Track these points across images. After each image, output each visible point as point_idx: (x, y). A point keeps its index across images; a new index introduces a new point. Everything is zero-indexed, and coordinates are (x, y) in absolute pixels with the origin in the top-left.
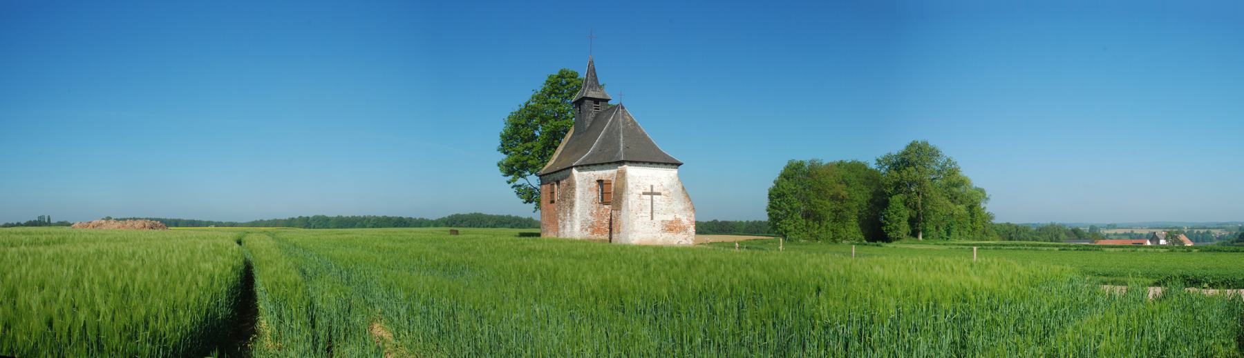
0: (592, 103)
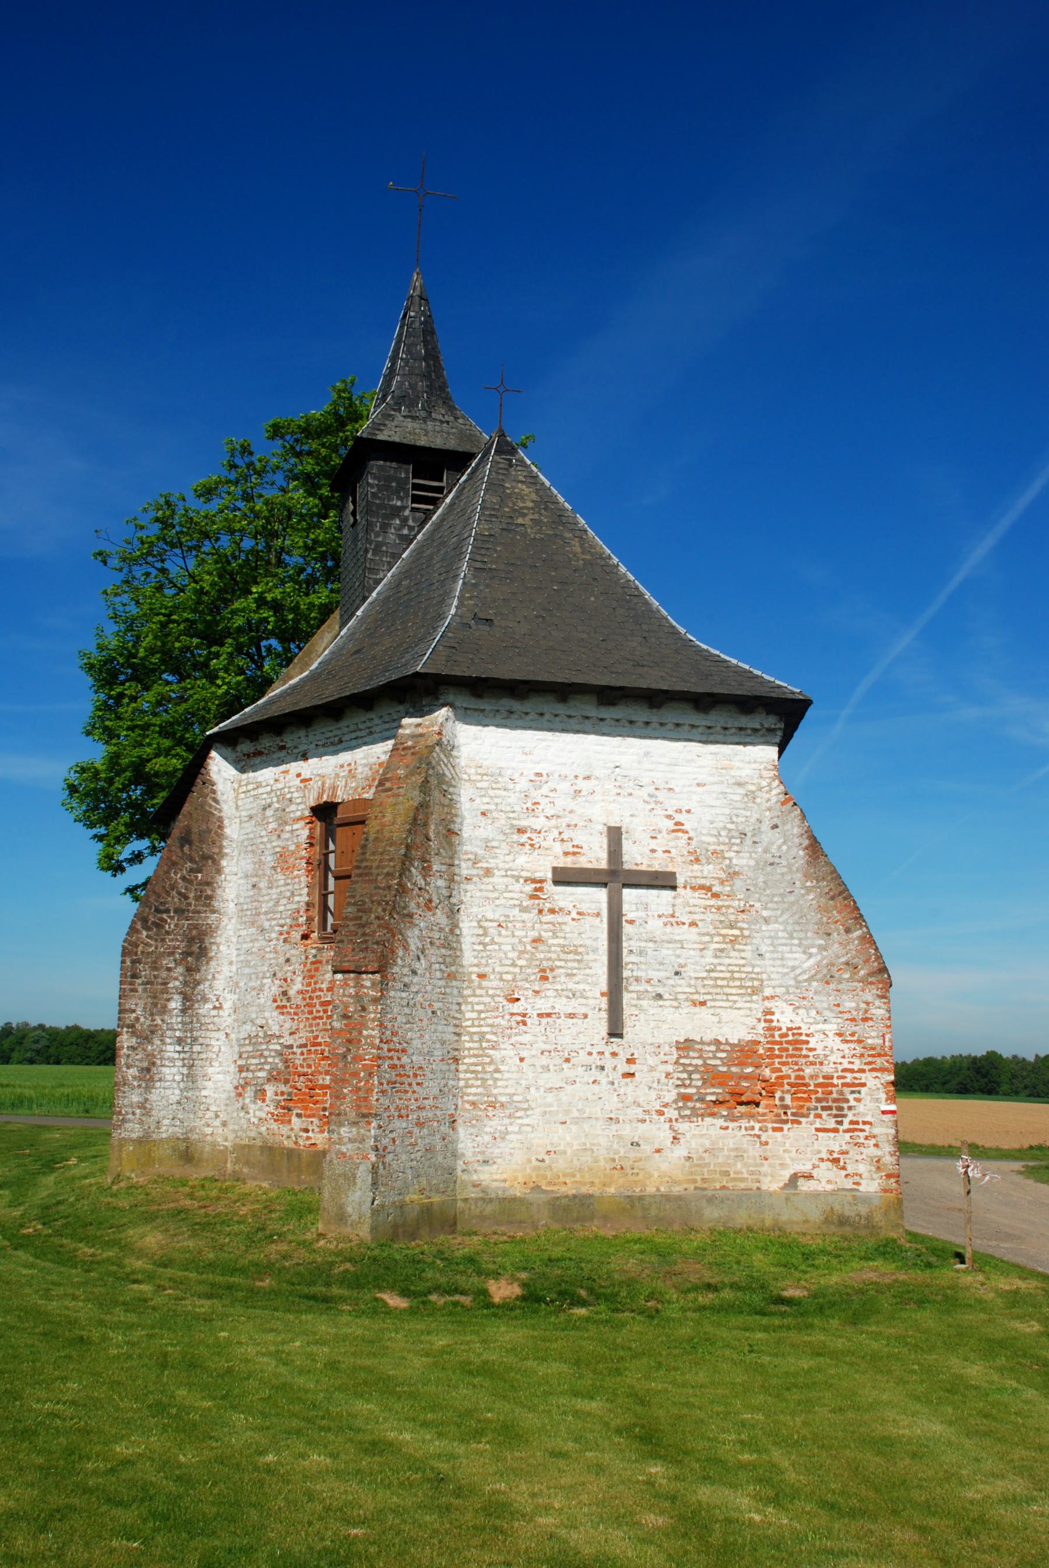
0: (405, 473)
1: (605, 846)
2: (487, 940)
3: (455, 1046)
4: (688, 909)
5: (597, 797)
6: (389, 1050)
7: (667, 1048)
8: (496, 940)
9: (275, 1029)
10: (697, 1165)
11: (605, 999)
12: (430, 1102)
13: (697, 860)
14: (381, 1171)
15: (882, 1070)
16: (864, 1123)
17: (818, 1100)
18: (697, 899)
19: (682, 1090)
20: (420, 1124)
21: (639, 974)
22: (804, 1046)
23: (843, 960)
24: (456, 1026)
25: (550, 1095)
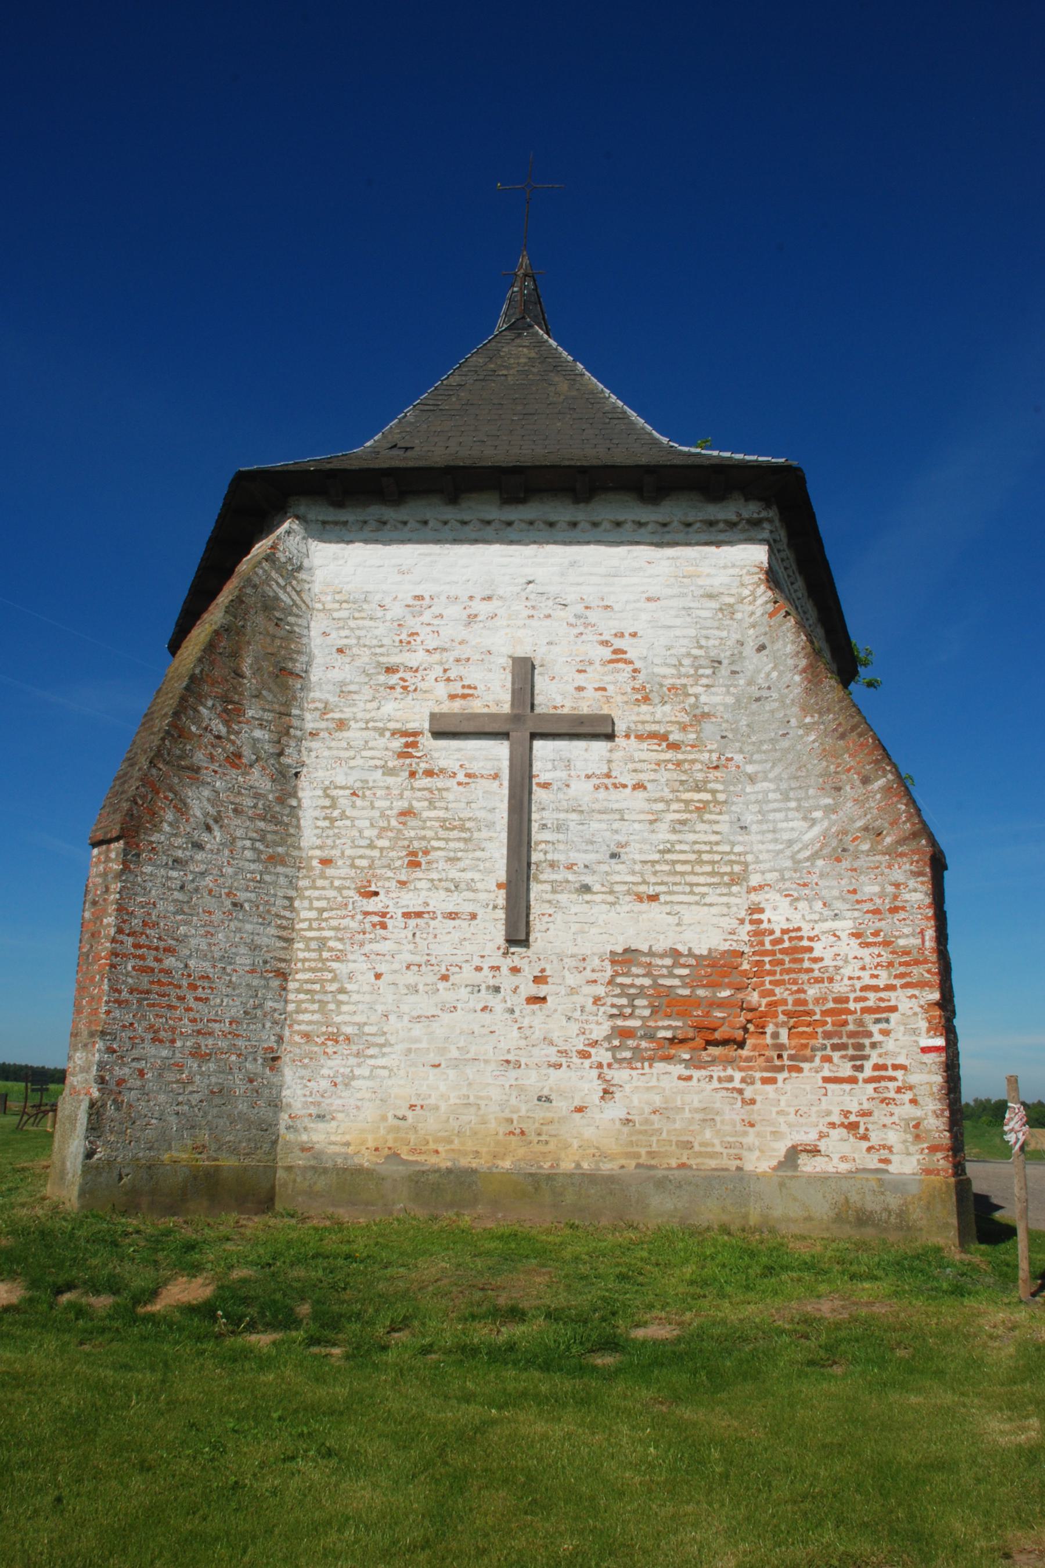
1: (509, 685)
2: (336, 813)
3: (281, 954)
4: (630, 766)
5: (498, 622)
6: (137, 946)
7: (596, 962)
8: (348, 813)
10: (640, 1132)
11: (503, 893)
12: (226, 1028)
13: (646, 699)
14: (110, 1110)
15: (921, 985)
16: (896, 1067)
17: (827, 1035)
18: (646, 752)
19: (620, 1022)
20: (196, 1053)
21: (556, 857)
22: (806, 956)
23: (860, 824)
24: (280, 927)
25: (418, 1025)
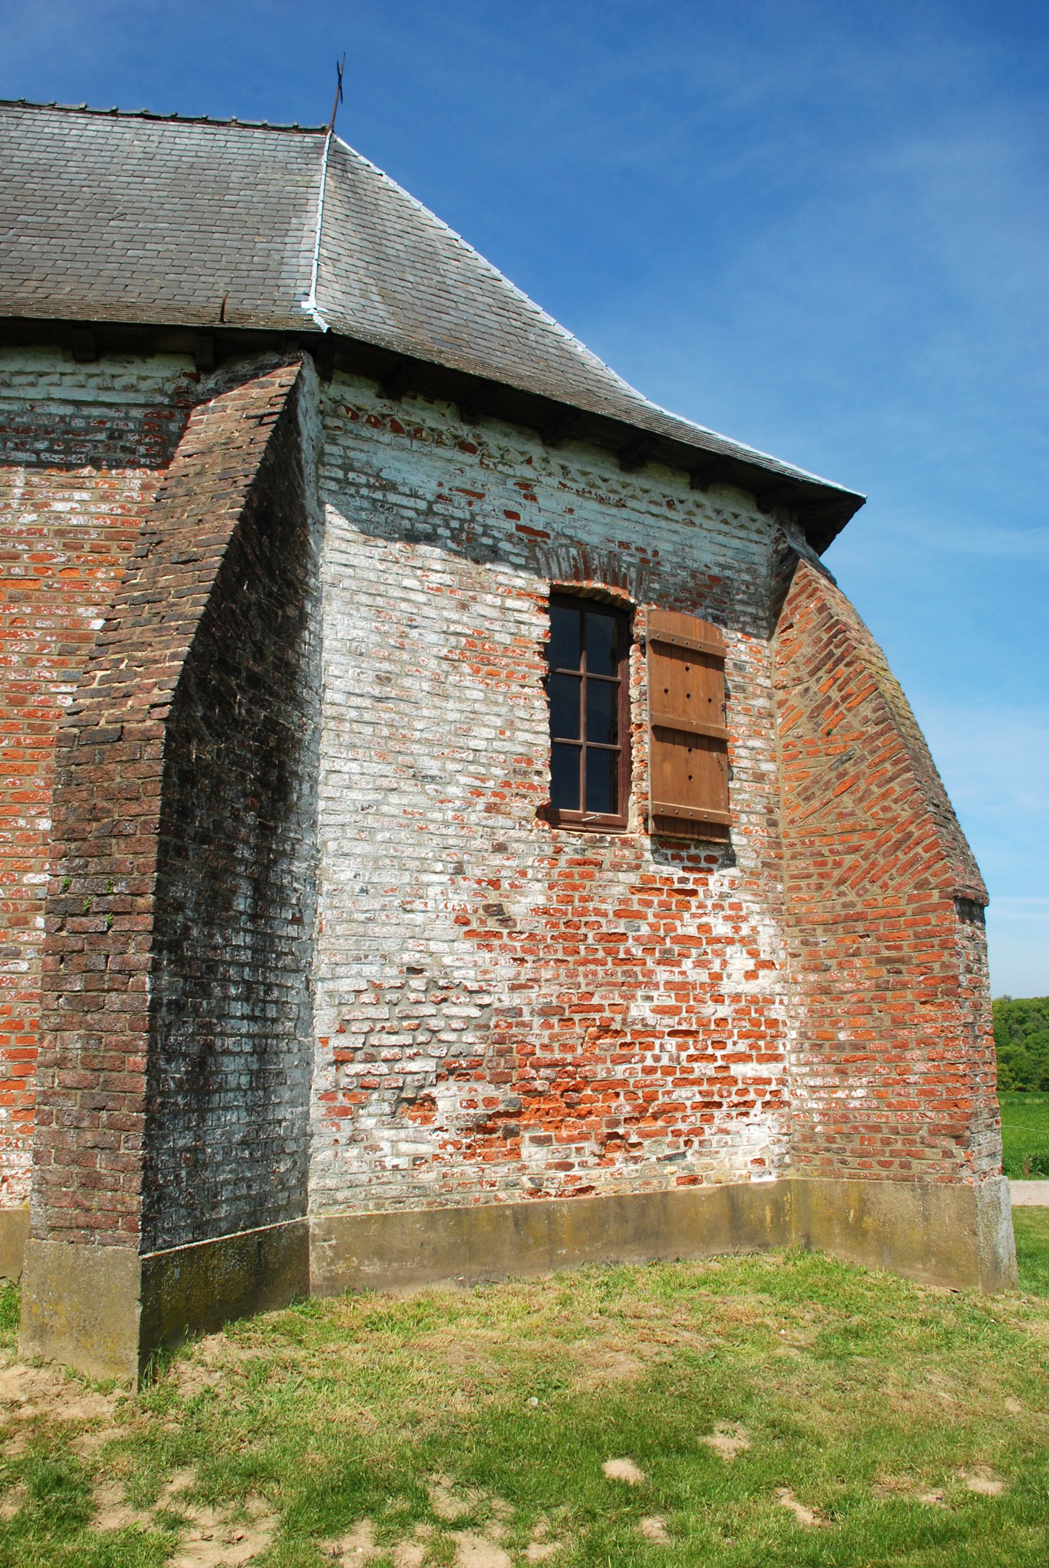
9: (468, 977)
